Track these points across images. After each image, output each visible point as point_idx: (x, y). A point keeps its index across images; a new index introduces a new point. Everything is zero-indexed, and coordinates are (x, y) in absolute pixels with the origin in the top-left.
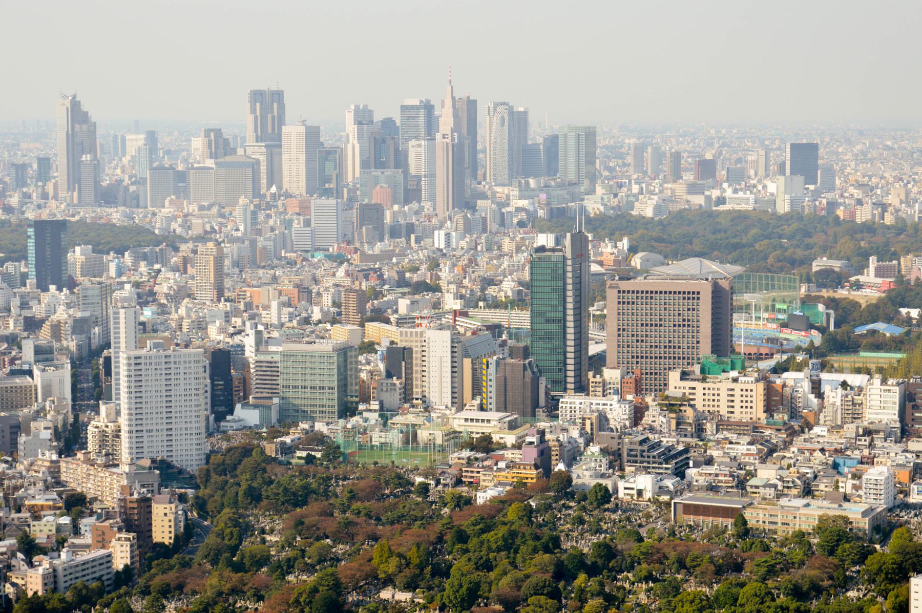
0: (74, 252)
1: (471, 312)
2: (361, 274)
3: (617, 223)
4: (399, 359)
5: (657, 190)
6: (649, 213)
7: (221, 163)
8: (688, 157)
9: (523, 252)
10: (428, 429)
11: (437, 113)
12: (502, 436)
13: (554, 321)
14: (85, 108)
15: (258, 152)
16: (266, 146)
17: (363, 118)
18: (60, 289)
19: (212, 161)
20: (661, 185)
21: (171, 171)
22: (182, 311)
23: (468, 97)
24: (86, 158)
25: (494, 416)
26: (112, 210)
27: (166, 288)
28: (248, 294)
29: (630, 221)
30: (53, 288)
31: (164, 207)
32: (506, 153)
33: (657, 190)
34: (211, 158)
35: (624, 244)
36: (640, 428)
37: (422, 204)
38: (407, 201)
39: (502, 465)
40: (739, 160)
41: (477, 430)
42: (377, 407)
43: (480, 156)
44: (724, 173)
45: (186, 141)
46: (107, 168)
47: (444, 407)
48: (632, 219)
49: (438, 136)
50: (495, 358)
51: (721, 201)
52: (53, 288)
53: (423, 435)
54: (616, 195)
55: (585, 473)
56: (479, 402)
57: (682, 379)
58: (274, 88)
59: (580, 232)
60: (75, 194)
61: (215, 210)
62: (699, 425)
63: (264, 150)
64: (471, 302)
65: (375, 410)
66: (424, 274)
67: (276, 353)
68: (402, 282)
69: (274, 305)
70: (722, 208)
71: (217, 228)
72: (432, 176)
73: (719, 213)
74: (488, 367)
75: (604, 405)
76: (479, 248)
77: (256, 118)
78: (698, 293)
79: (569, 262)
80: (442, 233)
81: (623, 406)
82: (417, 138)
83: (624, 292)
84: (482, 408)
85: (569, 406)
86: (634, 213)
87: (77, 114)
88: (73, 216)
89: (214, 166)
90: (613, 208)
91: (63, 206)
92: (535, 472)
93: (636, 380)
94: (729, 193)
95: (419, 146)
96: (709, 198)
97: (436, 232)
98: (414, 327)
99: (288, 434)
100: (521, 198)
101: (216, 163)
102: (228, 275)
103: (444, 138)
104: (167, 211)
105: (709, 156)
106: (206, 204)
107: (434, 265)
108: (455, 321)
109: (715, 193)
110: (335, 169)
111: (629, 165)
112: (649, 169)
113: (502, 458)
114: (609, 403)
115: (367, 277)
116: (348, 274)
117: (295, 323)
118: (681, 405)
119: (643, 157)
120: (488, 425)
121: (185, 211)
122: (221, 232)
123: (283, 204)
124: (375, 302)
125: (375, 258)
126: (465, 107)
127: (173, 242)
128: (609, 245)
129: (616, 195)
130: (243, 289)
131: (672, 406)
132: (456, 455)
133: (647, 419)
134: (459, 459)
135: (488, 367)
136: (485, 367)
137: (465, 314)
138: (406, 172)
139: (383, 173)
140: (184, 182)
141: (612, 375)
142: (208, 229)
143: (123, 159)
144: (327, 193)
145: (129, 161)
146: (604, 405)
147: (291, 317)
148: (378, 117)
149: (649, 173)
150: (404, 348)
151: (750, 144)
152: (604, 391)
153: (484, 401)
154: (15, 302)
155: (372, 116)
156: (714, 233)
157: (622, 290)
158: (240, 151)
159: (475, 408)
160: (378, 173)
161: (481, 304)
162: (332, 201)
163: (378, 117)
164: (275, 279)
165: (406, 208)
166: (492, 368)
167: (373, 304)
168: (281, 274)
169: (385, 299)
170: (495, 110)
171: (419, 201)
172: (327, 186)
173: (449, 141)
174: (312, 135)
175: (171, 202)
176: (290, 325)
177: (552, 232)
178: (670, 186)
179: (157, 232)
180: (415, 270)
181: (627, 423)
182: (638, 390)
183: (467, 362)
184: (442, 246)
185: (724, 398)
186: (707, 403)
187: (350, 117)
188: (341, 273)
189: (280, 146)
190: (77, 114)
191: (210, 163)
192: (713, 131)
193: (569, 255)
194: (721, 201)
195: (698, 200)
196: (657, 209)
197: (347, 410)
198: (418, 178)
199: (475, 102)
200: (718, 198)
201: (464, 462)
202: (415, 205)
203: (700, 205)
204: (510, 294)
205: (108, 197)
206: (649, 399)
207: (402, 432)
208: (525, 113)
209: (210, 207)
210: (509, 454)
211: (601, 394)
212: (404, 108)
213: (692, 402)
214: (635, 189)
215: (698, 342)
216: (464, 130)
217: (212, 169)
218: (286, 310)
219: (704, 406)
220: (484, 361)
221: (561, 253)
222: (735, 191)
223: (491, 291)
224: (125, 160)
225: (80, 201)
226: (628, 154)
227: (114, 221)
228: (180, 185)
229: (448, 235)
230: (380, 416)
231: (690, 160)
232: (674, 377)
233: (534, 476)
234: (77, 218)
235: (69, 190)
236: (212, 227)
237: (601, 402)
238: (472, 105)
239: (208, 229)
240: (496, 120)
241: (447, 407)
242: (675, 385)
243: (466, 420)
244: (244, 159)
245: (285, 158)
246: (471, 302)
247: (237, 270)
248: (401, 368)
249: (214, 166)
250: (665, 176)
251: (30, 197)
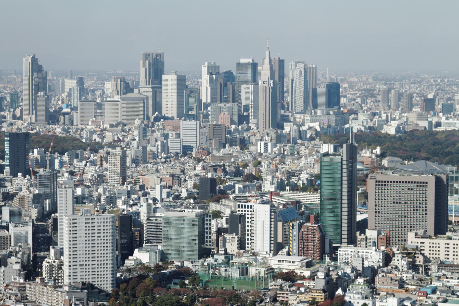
0: (33, 152)
1: (281, 193)
2: (212, 168)
3: (372, 137)
4: (238, 223)
5: (397, 118)
6: (392, 132)
7: (124, 98)
8: (417, 97)
9: (313, 155)
10: (255, 266)
11: (259, 68)
12: (302, 271)
13: (335, 199)
15: (147, 91)
16: (152, 88)
17: (213, 70)
18: (24, 176)
19: (119, 96)
20: (400, 114)
21: (93, 103)
22: (101, 190)
23: (279, 58)
24: (41, 94)
25: (297, 259)
27: (90, 175)
28: (141, 180)
29: (380, 137)
30: (20, 175)
31: (88, 125)
32: (302, 93)
33: (397, 118)
34: (118, 94)
35: (378, 150)
36: (389, 268)
37: (250, 125)
38: (240, 122)
39: (302, 290)
40: (449, 99)
41: (286, 268)
42: (223, 252)
43: (286, 95)
44: (440, 106)
45: (102, 84)
46: (52, 100)
47: (265, 253)
48: (382, 136)
49: (260, 82)
50: (298, 222)
51: (439, 124)
52: (20, 175)
53: (252, 271)
54: (371, 120)
55: (355, 295)
56: (287, 250)
57: (415, 237)
59: (352, 144)
60: (34, 116)
61: (120, 127)
62: (427, 266)
63: (151, 90)
64: (281, 186)
65: (222, 254)
66: (250, 170)
67: (161, 217)
68: (237, 173)
69: (158, 187)
70: (438, 129)
71: (121, 138)
72: (256, 107)
73: (437, 133)
74: (293, 228)
75: (366, 252)
76: (286, 153)
77: (146, 70)
78: (427, 183)
79: (345, 163)
80: (263, 143)
81: (378, 253)
82: (246, 83)
83: (379, 181)
84: (288, 254)
85: (344, 253)
86: (383, 132)
87: (36, 67)
88: (32, 130)
89: (119, 100)
90: (370, 128)
91: (26, 124)
92: (323, 295)
93: (387, 238)
94: (443, 120)
95: (248, 88)
96: (430, 123)
97: (259, 143)
98: (247, 202)
100: (312, 121)
101: (121, 98)
102: (129, 168)
103: (264, 83)
104: (90, 127)
105: (430, 96)
106: (114, 123)
108: (271, 198)
109: (435, 120)
110: (195, 102)
111: (379, 101)
112: (392, 103)
113: (302, 285)
114: (369, 251)
115: (215, 170)
116: (203, 168)
117: (171, 198)
118: (415, 254)
119: (388, 96)
120: (293, 264)
121: (102, 127)
122: (123, 141)
123: (163, 124)
124: (221, 186)
125: (219, 158)
126: (277, 64)
127: (95, 148)
128: (368, 152)
129: (371, 120)
130: (138, 177)
131: (410, 254)
132: (273, 283)
133: (394, 262)
134: (275, 285)
135: (293, 228)
136: (291, 228)
137: (278, 195)
138: (240, 103)
139: (225, 105)
140: (101, 109)
141: (371, 234)
142: (116, 139)
143: (63, 95)
144: (191, 117)
145: (67, 96)
146: (366, 252)
147: (169, 195)
148: (222, 70)
149: (392, 107)
150: (241, 215)
151: (456, 89)
152: (366, 244)
153: (291, 249)
155: (218, 69)
156: (434, 145)
157: (378, 180)
158: (136, 91)
159: (285, 254)
160: (222, 105)
161: (287, 188)
162: (194, 122)
163: (222, 70)
164: (157, 171)
165: (240, 127)
166: (296, 228)
167: (220, 187)
168: (162, 168)
169: (227, 184)
170: (296, 66)
171: (248, 123)
172: (190, 113)
173: (267, 85)
174: (181, 82)
175: (93, 122)
176: (168, 200)
177: (331, 143)
178: (406, 115)
179: (84, 140)
180: (246, 166)
181: (381, 265)
182: (388, 243)
183: (280, 224)
184: (262, 151)
185: (443, 249)
186: (432, 252)
187: (204, 70)
188: (199, 167)
189: (161, 88)
190: (36, 67)
191: (117, 98)
192: (432, 80)
193: (345, 158)
194: (439, 124)
195: (424, 124)
196: (398, 130)
197: (205, 253)
198: (247, 108)
199: (283, 61)
200: (437, 123)
201: (278, 287)
202: (245, 125)
203: (425, 128)
204: (305, 182)
205: (53, 118)
206: (395, 249)
207: (239, 268)
208: (315, 68)
209: (117, 125)
210: (306, 283)
211: (364, 245)
212: (239, 64)
213: (422, 252)
214: (384, 117)
215: (426, 214)
216: (276, 78)
217: (119, 101)
218: (165, 191)
219: (430, 254)
220: (291, 224)
221: (340, 157)
222: (447, 119)
223: (294, 180)
224: (64, 95)
225: (36, 121)
226: (378, 94)
227: (58, 134)
228: (98, 111)
229: (266, 145)
230: (226, 258)
231: (418, 99)
232: (411, 236)
233: (323, 297)
234: (34, 132)
235: (29, 113)
236: (118, 138)
237: (365, 251)
238: (281, 63)
239: (116, 139)
240: (297, 73)
241: (267, 253)
242: (412, 240)
243: (279, 261)
244: (138, 96)
245: (164, 95)
246: (281, 186)
247: (134, 165)
248: (238, 228)
249: (119, 100)
250: (402, 109)
251: (5, 118)
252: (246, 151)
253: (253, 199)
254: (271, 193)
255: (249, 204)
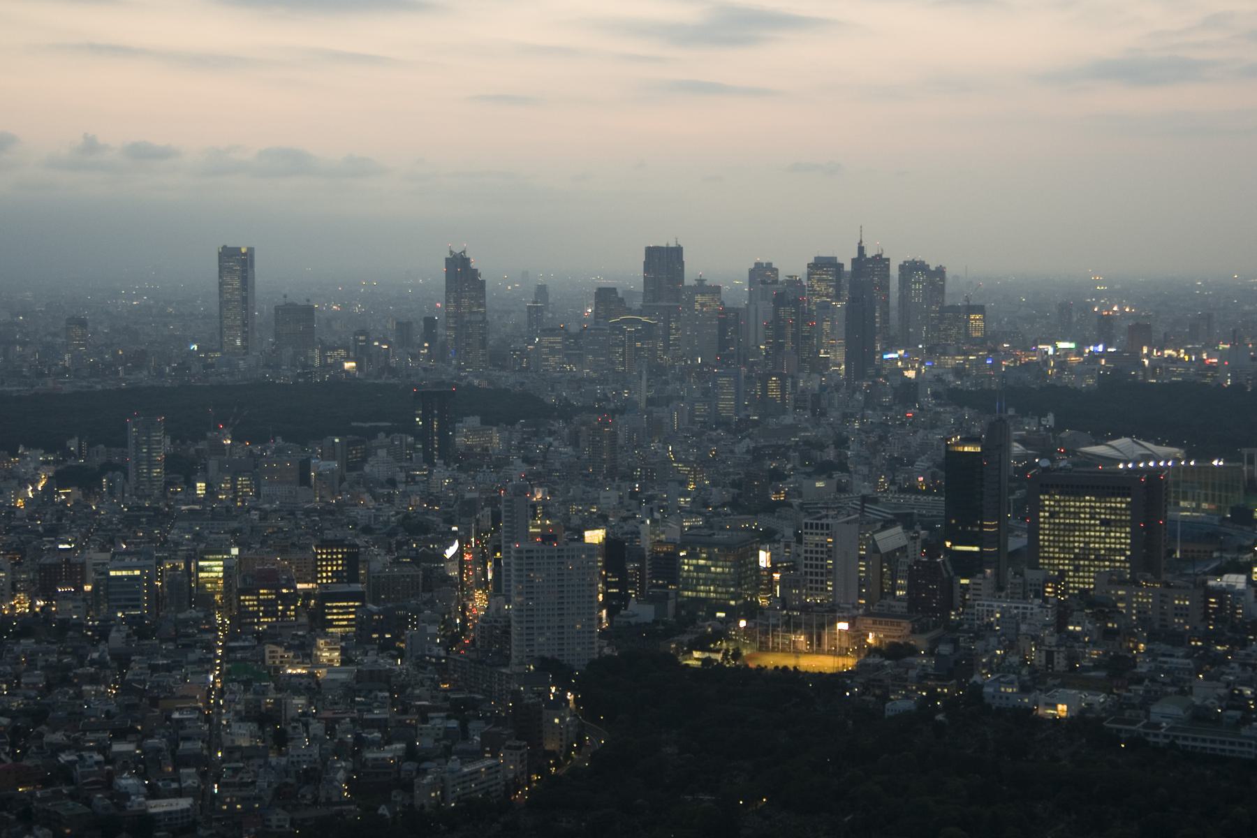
14: (473, 265)
26: (502, 373)
58: (672, 245)
66: (831, 454)
99: (684, 632)
107: (842, 443)
113: (913, 667)
127: (566, 411)
137: (875, 501)
148: (781, 277)
154: (401, 476)
163: (781, 277)
180: (821, 447)
234: (463, 383)
252: (823, 421)
253: (832, 513)
254: (865, 499)
255: (824, 521)
